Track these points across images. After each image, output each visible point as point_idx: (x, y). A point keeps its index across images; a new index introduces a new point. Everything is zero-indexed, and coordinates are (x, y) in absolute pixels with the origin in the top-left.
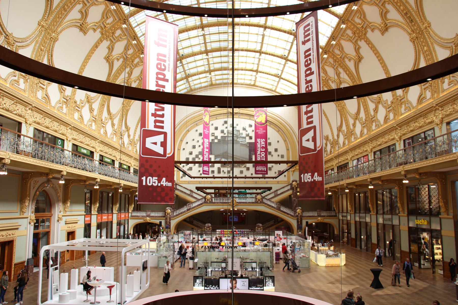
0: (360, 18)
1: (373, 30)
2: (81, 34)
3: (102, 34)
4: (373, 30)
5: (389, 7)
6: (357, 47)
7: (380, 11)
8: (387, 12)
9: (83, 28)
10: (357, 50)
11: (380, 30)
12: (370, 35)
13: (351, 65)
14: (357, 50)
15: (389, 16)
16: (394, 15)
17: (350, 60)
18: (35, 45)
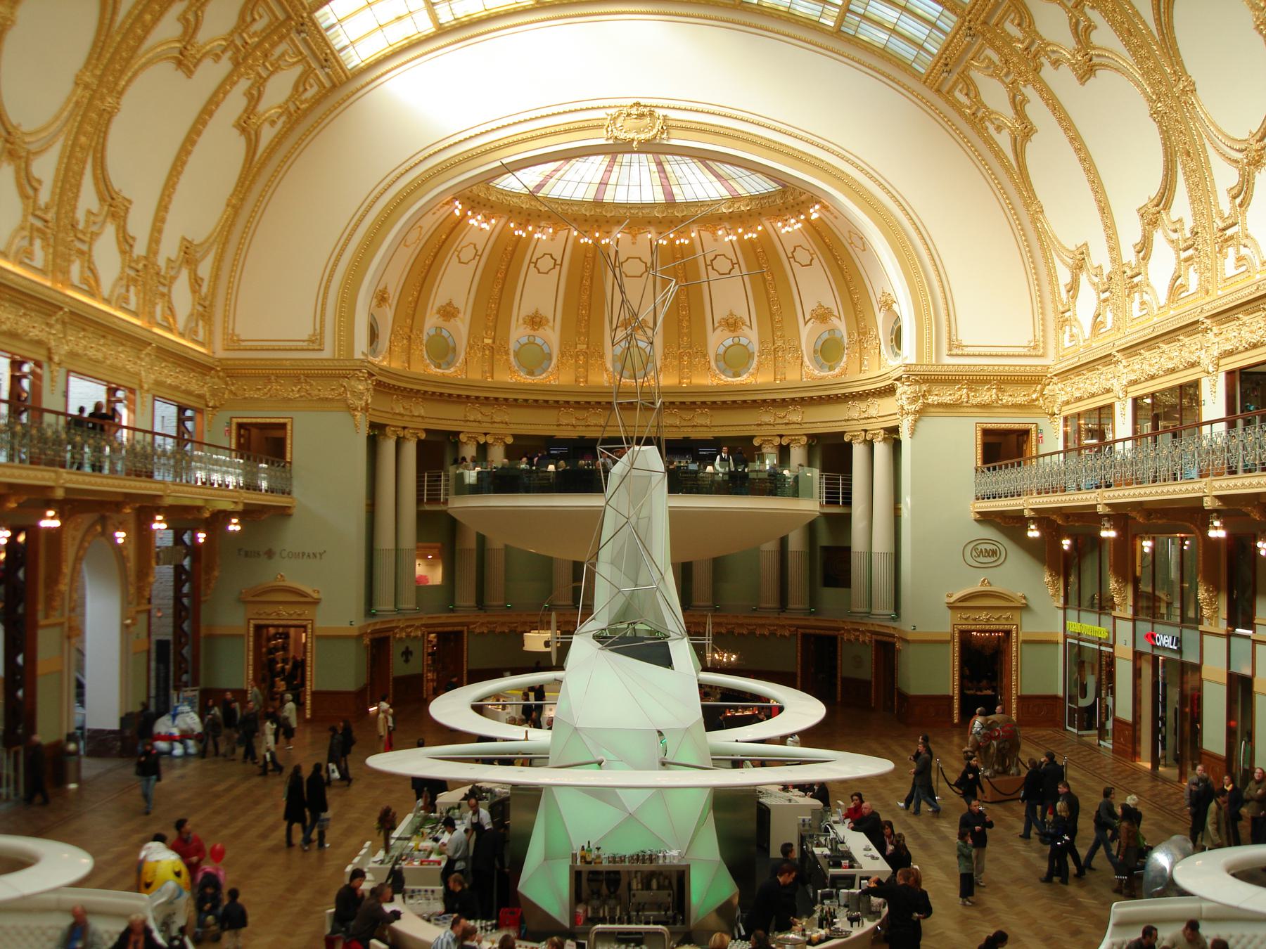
0: (1019, 25)
1: (1056, 64)
2: (180, 74)
3: (237, 64)
4: (1056, 64)
5: (1095, 16)
6: (1019, 98)
7: (1071, 19)
8: (1090, 27)
9: (185, 61)
10: (1018, 106)
11: (1074, 69)
12: (1047, 72)
13: (1004, 141)
14: (1018, 106)
15: (1095, 38)
16: (1105, 36)
17: (999, 129)
18: (66, 139)
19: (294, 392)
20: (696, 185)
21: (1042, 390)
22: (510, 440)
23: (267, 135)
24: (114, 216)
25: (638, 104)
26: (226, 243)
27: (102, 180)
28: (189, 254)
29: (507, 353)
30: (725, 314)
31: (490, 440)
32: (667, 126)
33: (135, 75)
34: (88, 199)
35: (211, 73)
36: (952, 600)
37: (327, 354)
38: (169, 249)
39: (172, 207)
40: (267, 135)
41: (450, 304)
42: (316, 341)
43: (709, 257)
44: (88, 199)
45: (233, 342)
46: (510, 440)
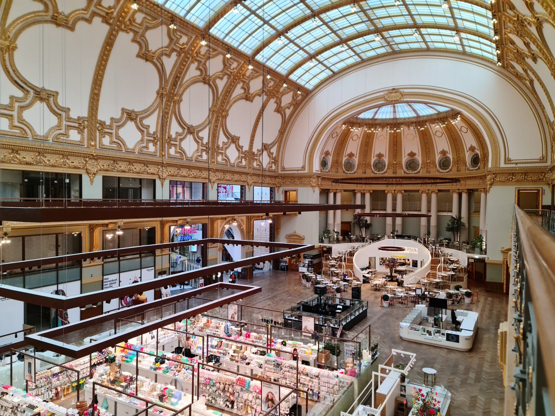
19: (298, 182)
20: (425, 111)
21: (544, 175)
22: (371, 192)
23: (288, 112)
24: (233, 142)
25: (394, 89)
26: (281, 141)
27: (227, 134)
28: (265, 147)
29: (371, 166)
30: (441, 150)
31: (365, 191)
32: (402, 95)
33: (231, 106)
34: (222, 139)
35: (258, 101)
36: (503, 250)
37: (306, 171)
38: (257, 146)
39: (256, 137)
40: (288, 112)
41: (351, 153)
42: (303, 168)
43: (434, 132)
44: (222, 139)
45: (283, 169)
46: (371, 192)
